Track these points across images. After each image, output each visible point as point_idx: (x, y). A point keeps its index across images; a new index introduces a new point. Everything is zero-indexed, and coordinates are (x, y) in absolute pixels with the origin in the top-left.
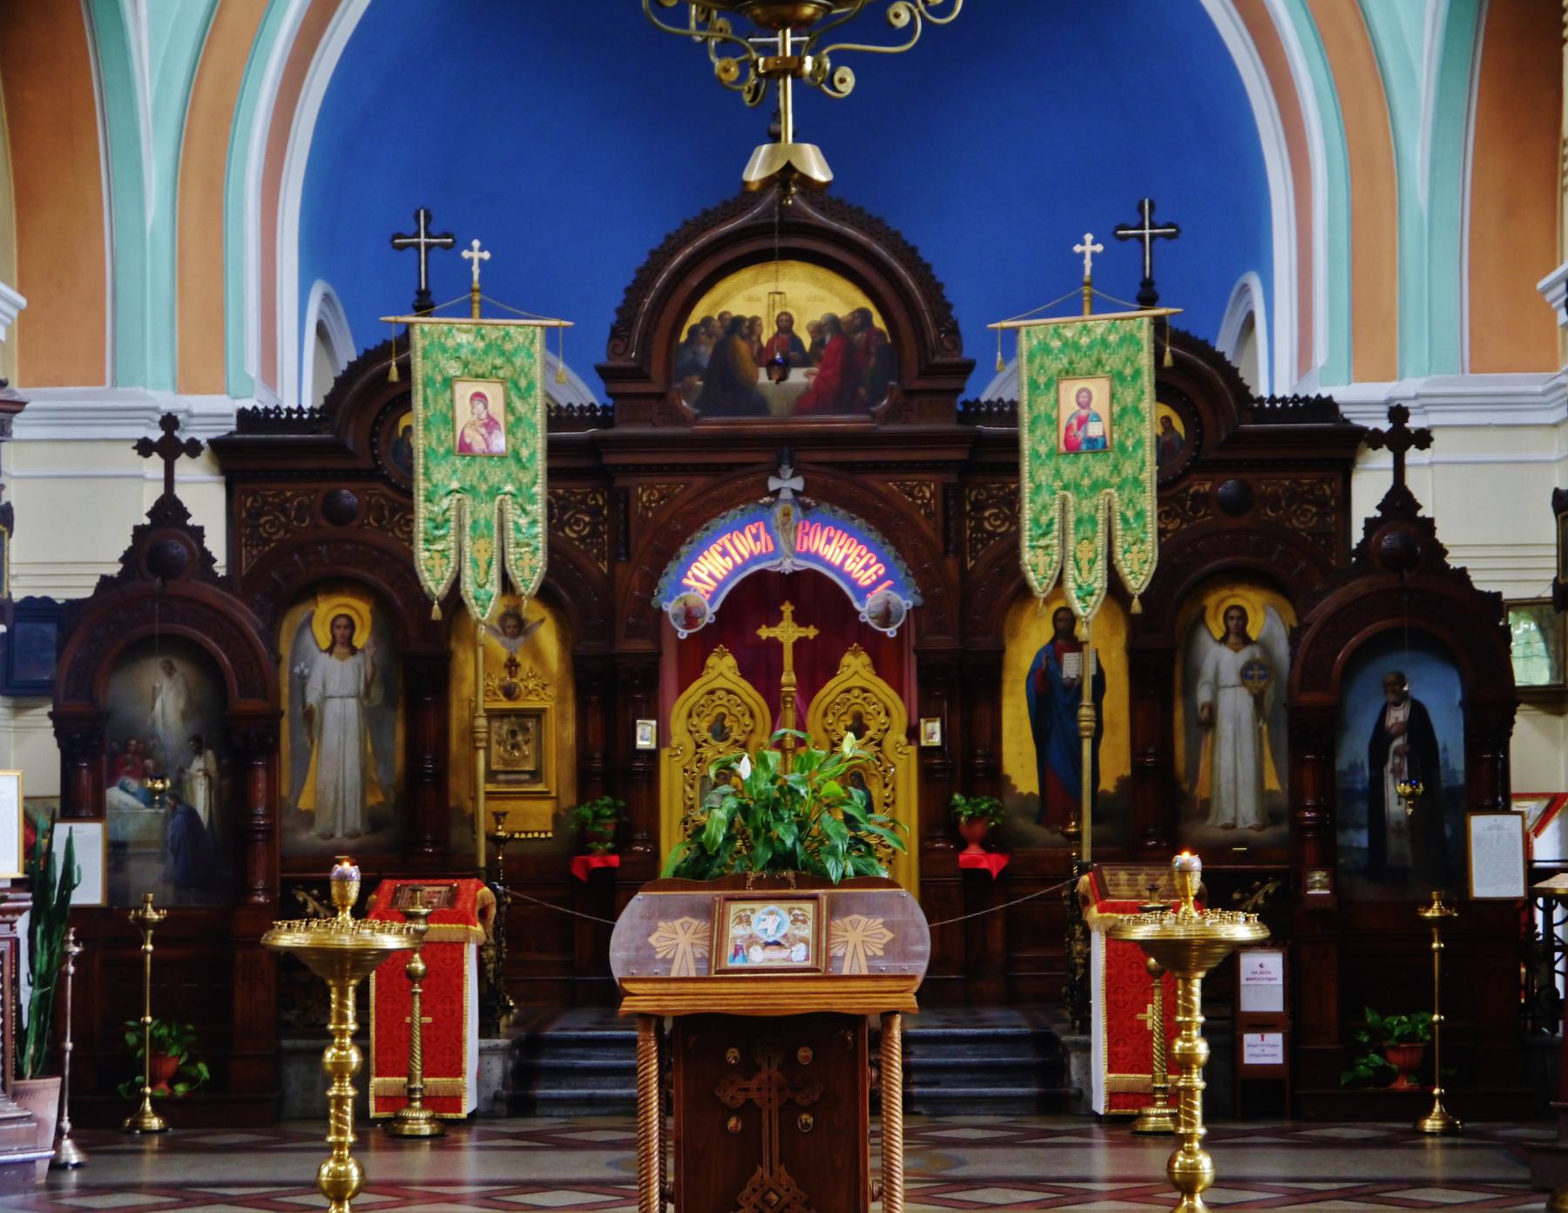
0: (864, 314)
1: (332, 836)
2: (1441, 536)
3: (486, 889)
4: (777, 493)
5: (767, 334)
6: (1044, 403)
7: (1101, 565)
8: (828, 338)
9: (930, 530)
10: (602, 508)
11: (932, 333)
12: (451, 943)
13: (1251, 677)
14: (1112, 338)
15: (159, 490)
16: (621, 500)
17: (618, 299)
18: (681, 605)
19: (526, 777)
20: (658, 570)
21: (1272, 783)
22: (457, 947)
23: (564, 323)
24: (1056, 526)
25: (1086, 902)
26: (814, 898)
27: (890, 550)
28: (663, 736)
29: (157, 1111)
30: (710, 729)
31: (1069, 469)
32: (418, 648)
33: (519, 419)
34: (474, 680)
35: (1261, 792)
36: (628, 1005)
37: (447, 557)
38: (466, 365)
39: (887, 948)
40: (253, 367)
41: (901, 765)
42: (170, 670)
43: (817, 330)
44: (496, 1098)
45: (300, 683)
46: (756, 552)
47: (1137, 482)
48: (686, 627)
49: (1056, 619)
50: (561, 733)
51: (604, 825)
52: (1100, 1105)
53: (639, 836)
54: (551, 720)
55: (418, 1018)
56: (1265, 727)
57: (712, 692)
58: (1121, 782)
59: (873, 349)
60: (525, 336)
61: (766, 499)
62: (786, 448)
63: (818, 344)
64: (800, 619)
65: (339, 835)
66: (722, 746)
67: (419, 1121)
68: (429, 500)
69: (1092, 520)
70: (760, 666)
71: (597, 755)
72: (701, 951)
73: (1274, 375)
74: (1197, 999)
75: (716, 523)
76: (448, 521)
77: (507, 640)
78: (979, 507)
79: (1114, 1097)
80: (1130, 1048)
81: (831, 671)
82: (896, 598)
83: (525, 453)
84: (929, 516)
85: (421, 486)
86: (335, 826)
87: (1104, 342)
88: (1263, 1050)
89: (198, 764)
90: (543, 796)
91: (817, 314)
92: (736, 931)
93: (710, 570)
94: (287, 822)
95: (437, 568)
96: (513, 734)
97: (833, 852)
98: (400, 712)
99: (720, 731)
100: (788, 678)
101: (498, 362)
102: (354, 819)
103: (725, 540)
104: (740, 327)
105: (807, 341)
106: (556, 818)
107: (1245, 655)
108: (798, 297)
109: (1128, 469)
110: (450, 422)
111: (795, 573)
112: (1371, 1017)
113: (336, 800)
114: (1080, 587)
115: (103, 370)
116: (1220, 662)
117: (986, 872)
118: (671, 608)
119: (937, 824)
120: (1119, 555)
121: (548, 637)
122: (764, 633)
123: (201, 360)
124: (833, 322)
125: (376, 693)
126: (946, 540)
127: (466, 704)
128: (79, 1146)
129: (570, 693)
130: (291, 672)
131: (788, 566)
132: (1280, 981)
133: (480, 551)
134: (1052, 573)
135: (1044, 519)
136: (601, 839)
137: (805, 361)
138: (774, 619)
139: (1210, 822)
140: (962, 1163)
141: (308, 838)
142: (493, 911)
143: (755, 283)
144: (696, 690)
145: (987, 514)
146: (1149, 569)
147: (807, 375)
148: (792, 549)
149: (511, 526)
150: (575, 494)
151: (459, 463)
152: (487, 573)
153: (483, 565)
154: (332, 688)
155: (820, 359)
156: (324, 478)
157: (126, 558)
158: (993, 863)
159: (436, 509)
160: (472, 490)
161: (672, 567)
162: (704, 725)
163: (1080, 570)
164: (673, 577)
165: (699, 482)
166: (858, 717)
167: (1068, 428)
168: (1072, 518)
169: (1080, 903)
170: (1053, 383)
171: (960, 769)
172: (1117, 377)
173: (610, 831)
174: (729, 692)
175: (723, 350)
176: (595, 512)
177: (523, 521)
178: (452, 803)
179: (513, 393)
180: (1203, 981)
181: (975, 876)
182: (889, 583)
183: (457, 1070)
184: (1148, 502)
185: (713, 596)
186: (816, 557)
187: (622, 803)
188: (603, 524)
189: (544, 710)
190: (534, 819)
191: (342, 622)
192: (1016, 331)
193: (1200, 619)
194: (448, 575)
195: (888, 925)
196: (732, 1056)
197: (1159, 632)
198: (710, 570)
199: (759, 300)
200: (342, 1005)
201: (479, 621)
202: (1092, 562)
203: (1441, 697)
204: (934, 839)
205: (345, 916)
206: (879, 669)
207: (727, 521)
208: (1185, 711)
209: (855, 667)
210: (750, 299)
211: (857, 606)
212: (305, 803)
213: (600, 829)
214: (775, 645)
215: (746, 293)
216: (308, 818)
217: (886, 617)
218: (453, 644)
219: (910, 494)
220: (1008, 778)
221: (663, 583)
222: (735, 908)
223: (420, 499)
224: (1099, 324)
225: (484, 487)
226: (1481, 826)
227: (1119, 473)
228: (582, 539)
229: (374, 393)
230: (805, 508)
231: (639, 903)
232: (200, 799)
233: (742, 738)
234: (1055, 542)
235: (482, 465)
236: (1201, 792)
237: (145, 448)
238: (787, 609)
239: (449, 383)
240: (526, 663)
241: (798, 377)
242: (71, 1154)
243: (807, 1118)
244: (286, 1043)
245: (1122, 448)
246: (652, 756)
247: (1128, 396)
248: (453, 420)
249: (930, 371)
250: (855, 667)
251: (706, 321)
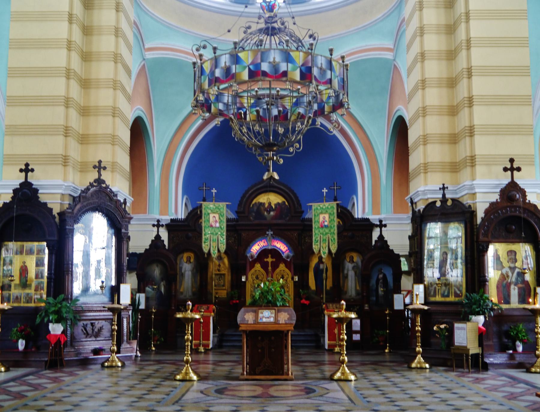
0: (284, 202)
2: (389, 243)
5: (266, 205)
6: (317, 219)
7: (327, 248)
11: (296, 205)
14: (329, 207)
15: (156, 233)
17: (239, 199)
21: (358, 288)
22: (209, 317)
25: (324, 310)
26: (275, 309)
28: (247, 279)
29: (154, 346)
31: (321, 231)
32: (202, 261)
33: (221, 221)
34: (213, 268)
36: (240, 329)
39: (288, 319)
40: (173, 211)
41: (290, 284)
42: (157, 266)
43: (275, 205)
44: (216, 345)
45: (181, 268)
47: (334, 233)
49: (319, 258)
50: (228, 278)
52: (327, 347)
55: (202, 330)
58: (331, 288)
60: (223, 205)
62: (270, 226)
64: (272, 257)
67: (202, 349)
68: (205, 235)
70: (265, 266)
72: (254, 319)
73: (358, 214)
74: (345, 328)
75: (257, 240)
79: (329, 346)
80: (332, 337)
82: (290, 254)
85: (203, 232)
87: (328, 207)
88: (356, 337)
89: (162, 283)
90: (225, 289)
91: (275, 202)
92: (260, 315)
93: (256, 248)
97: (278, 301)
99: (257, 278)
100: (270, 268)
102: (190, 294)
103: (258, 243)
104: (262, 204)
105: (274, 207)
106: (227, 294)
107: (353, 265)
108: (273, 199)
109: (332, 231)
110: (209, 221)
112: (376, 331)
116: (349, 266)
118: (248, 255)
119: (297, 295)
121: (226, 261)
122: (265, 260)
123: (164, 210)
124: (278, 203)
125: (195, 270)
128: (140, 353)
131: (270, 248)
132: (359, 324)
133: (214, 244)
134: (318, 250)
137: (273, 210)
138: (267, 257)
140: (301, 358)
141: (182, 297)
144: (253, 271)
146: (336, 249)
154: (187, 269)
156: (186, 231)
157: (150, 246)
158: (307, 302)
160: (213, 234)
161: (249, 248)
162: (254, 277)
169: (323, 310)
170: (318, 215)
171: (301, 286)
172: (330, 214)
177: (222, 239)
180: (346, 326)
181: (304, 305)
183: (209, 340)
184: (336, 237)
186: (275, 246)
190: (223, 294)
193: (345, 258)
195: (288, 314)
196: (260, 338)
197: (338, 260)
198: (256, 248)
200: (188, 328)
203: (389, 273)
205: (189, 312)
206: (286, 267)
209: (282, 267)
212: (181, 290)
214: (268, 262)
216: (182, 293)
217: (288, 257)
221: (247, 251)
222: (260, 311)
223: (203, 235)
224: (327, 204)
226: (396, 296)
229: (195, 216)
230: (273, 237)
231: (243, 310)
232: (163, 290)
236: (345, 289)
237: (154, 225)
238: (270, 256)
239: (209, 214)
240: (222, 265)
241: (272, 213)
242: (139, 355)
243: (273, 350)
244: (178, 335)
245: (331, 227)
246: (245, 282)
247: (332, 218)
250: (282, 267)
251: (256, 203)
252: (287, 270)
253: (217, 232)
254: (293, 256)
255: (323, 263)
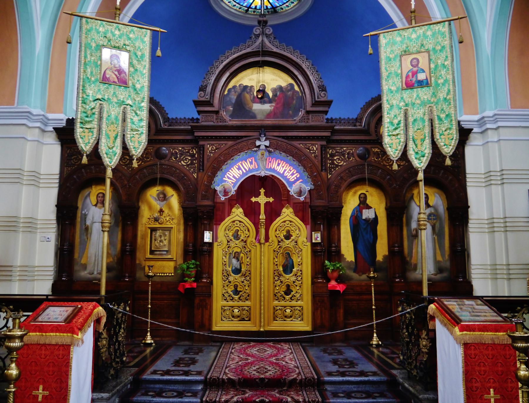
0: (291, 85)
1: (93, 274)
3: (100, 308)
4: (259, 146)
7: (428, 141)
8: (278, 93)
9: (317, 162)
10: (195, 154)
12: (63, 345)
13: (431, 219)
16: (202, 150)
18: (222, 187)
19: (165, 253)
20: (214, 174)
21: (439, 258)
23: (161, 30)
24: (402, 125)
25: (433, 318)
27: (301, 168)
28: (215, 237)
30: (233, 235)
35: (436, 262)
37: (92, 132)
38: (109, 41)
41: (304, 250)
43: (274, 91)
46: (251, 168)
48: (224, 196)
49: (360, 197)
50: (178, 236)
51: (191, 271)
53: (204, 276)
54: (174, 232)
56: (436, 238)
57: (234, 222)
58: (385, 257)
59: (295, 98)
61: (255, 149)
62: (262, 129)
63: (275, 95)
64: (267, 195)
65: (95, 273)
66: (237, 242)
69: (423, 120)
70: (251, 212)
71: (191, 245)
75: (236, 157)
76: (94, 114)
77: (159, 202)
78: (332, 155)
81: (279, 215)
82: (304, 186)
83: (138, 86)
84: (315, 157)
86: (94, 270)
90: (171, 260)
91: (274, 85)
94: (76, 268)
95: (86, 137)
96: (161, 236)
98: (120, 228)
99: (236, 236)
100: (262, 216)
101: (127, 43)
103: (239, 164)
105: (271, 95)
106: (175, 268)
111: (266, 177)
113: (95, 260)
114: (417, 153)
115: (14, 100)
117: (339, 291)
118: (218, 188)
119: (319, 272)
120: (437, 136)
121: (175, 201)
122: (254, 199)
124: (280, 88)
126: (322, 166)
127: (144, 225)
129: (182, 222)
130: (81, 213)
131: (263, 174)
134: (401, 147)
135: (396, 121)
136: (189, 277)
137: (270, 101)
138: (258, 195)
139: (417, 272)
141: (84, 274)
142: (104, 320)
143: (252, 74)
144: (227, 221)
145: (335, 158)
147: (270, 106)
148: (265, 167)
149: (129, 120)
150: (186, 149)
151: (103, 87)
152: (114, 142)
153: (112, 139)
155: (275, 101)
158: (341, 288)
159: (88, 107)
161: (219, 173)
162: (230, 234)
163: (416, 145)
164: (219, 177)
165: (230, 143)
166: (288, 232)
167: (407, 77)
168: (411, 120)
171: (325, 252)
173: (193, 274)
174: (240, 222)
175: (240, 97)
176: (193, 156)
177: (136, 119)
178: (137, 262)
179: (133, 57)
181: (334, 293)
182: (301, 180)
185: (235, 184)
186: (274, 170)
187: (198, 263)
188: (195, 160)
189: (172, 228)
191: (101, 195)
192: (377, 36)
194: (92, 141)
199: (253, 80)
201: (108, 166)
202: (423, 140)
204: (318, 278)
206: (296, 213)
207: (240, 157)
208: (407, 231)
209: (287, 213)
210: (250, 80)
211: (289, 189)
212: (83, 261)
213: (189, 273)
214: (258, 204)
215: (249, 77)
216: (85, 267)
217: (300, 193)
218: (140, 204)
219: (308, 149)
220: (343, 255)
221: (216, 179)
225: (115, 100)
227: (436, 96)
228: (188, 166)
230: (270, 152)
233: (245, 239)
234: (402, 132)
235: (114, 88)
236: (413, 261)
238: (262, 191)
240: (166, 211)
241: (267, 107)
245: (437, 85)
246: (211, 245)
248: (101, 65)
249: (316, 103)
250: (287, 213)
251: (234, 87)
252: (298, 221)
253: (121, 97)
254: (310, 191)
255: (369, 207)
